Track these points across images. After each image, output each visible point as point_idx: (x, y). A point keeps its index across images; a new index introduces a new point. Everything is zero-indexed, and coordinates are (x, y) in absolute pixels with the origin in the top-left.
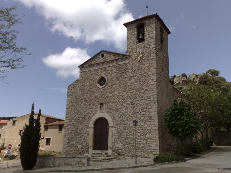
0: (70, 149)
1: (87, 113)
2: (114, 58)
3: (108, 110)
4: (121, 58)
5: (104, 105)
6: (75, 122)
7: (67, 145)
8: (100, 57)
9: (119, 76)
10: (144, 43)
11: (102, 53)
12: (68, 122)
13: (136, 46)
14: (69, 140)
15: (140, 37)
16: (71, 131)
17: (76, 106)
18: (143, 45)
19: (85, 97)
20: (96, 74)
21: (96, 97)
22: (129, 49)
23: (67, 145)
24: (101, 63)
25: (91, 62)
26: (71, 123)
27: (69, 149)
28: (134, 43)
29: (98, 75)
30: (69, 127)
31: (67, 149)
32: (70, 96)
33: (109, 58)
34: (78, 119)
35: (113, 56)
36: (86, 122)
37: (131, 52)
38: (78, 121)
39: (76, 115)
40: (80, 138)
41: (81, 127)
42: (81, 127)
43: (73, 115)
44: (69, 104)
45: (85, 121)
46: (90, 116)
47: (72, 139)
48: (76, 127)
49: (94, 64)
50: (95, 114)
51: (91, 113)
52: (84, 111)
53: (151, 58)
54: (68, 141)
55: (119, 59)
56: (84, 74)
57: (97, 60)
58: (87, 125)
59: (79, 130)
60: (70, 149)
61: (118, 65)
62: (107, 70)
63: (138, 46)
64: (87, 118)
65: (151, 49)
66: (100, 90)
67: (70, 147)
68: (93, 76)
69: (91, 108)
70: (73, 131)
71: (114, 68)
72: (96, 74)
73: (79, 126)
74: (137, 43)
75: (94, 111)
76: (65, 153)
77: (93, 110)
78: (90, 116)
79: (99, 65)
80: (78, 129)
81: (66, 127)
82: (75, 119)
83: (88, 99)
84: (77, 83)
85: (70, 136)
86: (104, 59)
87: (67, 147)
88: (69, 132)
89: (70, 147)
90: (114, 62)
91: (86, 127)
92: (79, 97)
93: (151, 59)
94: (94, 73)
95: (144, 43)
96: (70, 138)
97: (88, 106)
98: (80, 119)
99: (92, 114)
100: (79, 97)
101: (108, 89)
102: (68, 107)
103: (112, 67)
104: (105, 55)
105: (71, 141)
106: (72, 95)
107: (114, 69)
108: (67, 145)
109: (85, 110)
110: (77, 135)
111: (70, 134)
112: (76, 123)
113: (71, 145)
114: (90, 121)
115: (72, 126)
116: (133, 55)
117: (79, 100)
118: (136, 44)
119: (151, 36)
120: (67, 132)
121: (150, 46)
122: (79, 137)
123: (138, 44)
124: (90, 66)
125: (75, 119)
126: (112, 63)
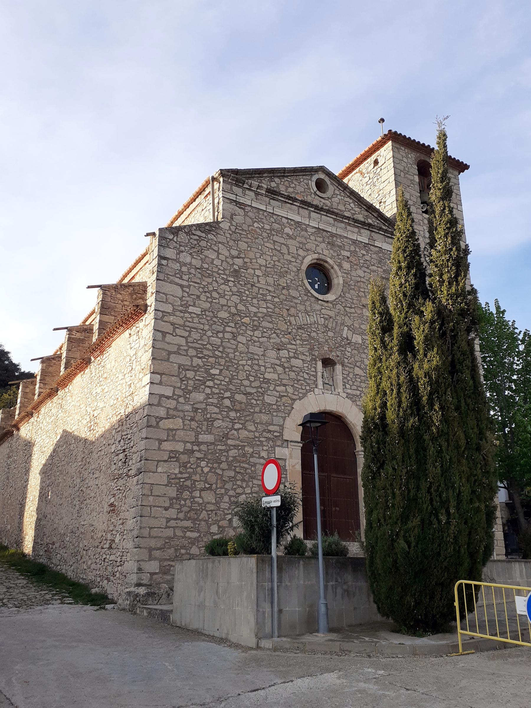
0: (189, 534)
1: (268, 381)
2: (360, 218)
3: (355, 392)
5: (338, 367)
6: (212, 404)
7: (166, 509)
11: (322, 176)
12: (168, 398)
14: (181, 489)
16: (189, 446)
17: (209, 333)
19: (254, 310)
21: (300, 328)
23: (172, 513)
24: (322, 209)
26: (188, 408)
27: (179, 533)
30: (178, 423)
31: (170, 532)
32: (177, 280)
33: (341, 207)
34: (228, 394)
35: (357, 210)
36: (264, 418)
38: (227, 402)
39: (212, 377)
40: (243, 480)
41: (244, 434)
42: (244, 434)
43: (195, 369)
44: (173, 314)
45: (261, 412)
46: (281, 397)
47: (200, 485)
48: (214, 431)
49: (295, 200)
50: (305, 395)
51: (285, 385)
52: (256, 367)
54: (172, 492)
55: (380, 229)
56: (241, 212)
57: (300, 189)
58: (271, 428)
59: (235, 447)
60: (189, 534)
61: (374, 246)
62: (340, 247)
64: (269, 399)
66: (318, 307)
67: (188, 524)
68: (282, 240)
69: (286, 365)
70: (203, 448)
71: (364, 252)
72: (298, 239)
73: (233, 428)
75: (298, 381)
76: (157, 554)
77: (293, 375)
78: (281, 397)
79: (307, 212)
80: (230, 442)
81: (162, 419)
82: (208, 391)
83: (271, 326)
84: (210, 236)
85: (184, 465)
87: (168, 520)
88: (180, 447)
89: (188, 524)
90: (362, 231)
91: (268, 439)
92: (223, 301)
96: (187, 479)
97: (272, 354)
98: (238, 397)
99: (290, 390)
100: (223, 301)
101: (346, 314)
102: (168, 328)
103: (354, 242)
104: (331, 189)
105: (192, 489)
106: (185, 277)
107: (364, 255)
108: (172, 513)
109: (258, 365)
110: (224, 466)
111: (184, 458)
112: (216, 410)
113: (192, 514)
114: (284, 419)
115: (192, 419)
117: (223, 314)
120: (167, 446)
122: (233, 479)
124: (272, 193)
125: (208, 391)
126: (356, 230)
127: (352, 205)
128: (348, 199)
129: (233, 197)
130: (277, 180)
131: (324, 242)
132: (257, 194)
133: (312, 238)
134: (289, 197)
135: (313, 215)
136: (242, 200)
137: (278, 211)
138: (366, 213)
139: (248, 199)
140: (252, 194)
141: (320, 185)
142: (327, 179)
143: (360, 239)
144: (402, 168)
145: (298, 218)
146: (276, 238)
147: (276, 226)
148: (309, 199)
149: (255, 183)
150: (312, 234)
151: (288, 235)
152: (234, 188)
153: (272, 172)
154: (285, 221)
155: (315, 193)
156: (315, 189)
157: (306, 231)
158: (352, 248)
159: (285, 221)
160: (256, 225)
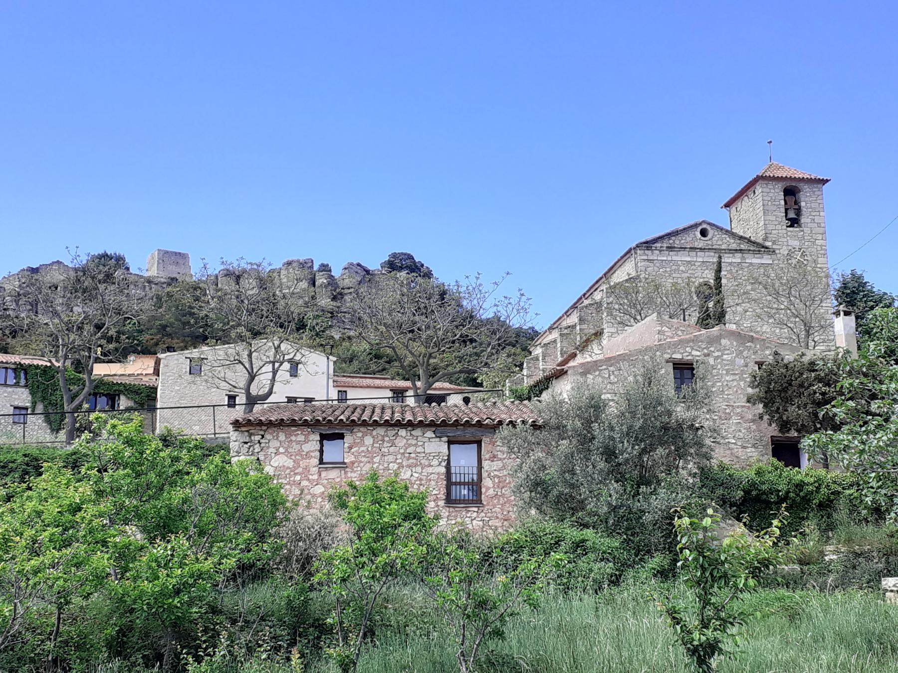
4: (754, 251)
8: (699, 235)
9: (749, 287)
10: (803, 231)
11: (704, 226)
13: (785, 232)
15: (792, 215)
18: (802, 233)
20: (690, 272)
22: (771, 234)
25: (671, 241)
28: (779, 224)
29: (696, 275)
37: (774, 243)
49: (685, 248)
53: (819, 266)
57: (689, 239)
63: (789, 233)
65: (819, 248)
68: (679, 275)
72: (690, 272)
74: (787, 227)
79: (695, 253)
86: (709, 242)
90: (736, 255)
93: (820, 268)
94: (682, 268)
95: (803, 231)
104: (711, 232)
116: (779, 249)
118: (785, 227)
119: (816, 221)
121: (816, 239)
123: (789, 229)
124: (670, 248)
126: (731, 255)
127: (728, 239)
128: (725, 236)
129: (645, 257)
130: (673, 238)
131: (707, 269)
132: (660, 251)
133: (699, 268)
134: (681, 248)
135: (699, 254)
136: (651, 258)
137: (674, 258)
138: (739, 241)
139: (655, 255)
140: (657, 252)
141: (704, 233)
142: (708, 228)
143: (734, 261)
144: (769, 199)
145: (688, 259)
146: (674, 275)
147: (674, 267)
148: (696, 245)
149: (658, 245)
150: (699, 266)
151: (682, 271)
152: (646, 252)
153: (669, 235)
154: (679, 262)
155: (700, 239)
156: (700, 236)
157: (695, 265)
158: (729, 268)
159: (679, 262)
160: (661, 270)
